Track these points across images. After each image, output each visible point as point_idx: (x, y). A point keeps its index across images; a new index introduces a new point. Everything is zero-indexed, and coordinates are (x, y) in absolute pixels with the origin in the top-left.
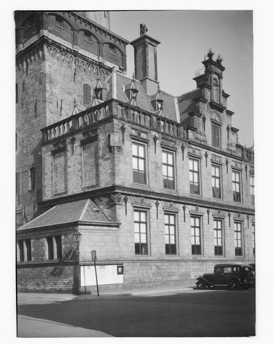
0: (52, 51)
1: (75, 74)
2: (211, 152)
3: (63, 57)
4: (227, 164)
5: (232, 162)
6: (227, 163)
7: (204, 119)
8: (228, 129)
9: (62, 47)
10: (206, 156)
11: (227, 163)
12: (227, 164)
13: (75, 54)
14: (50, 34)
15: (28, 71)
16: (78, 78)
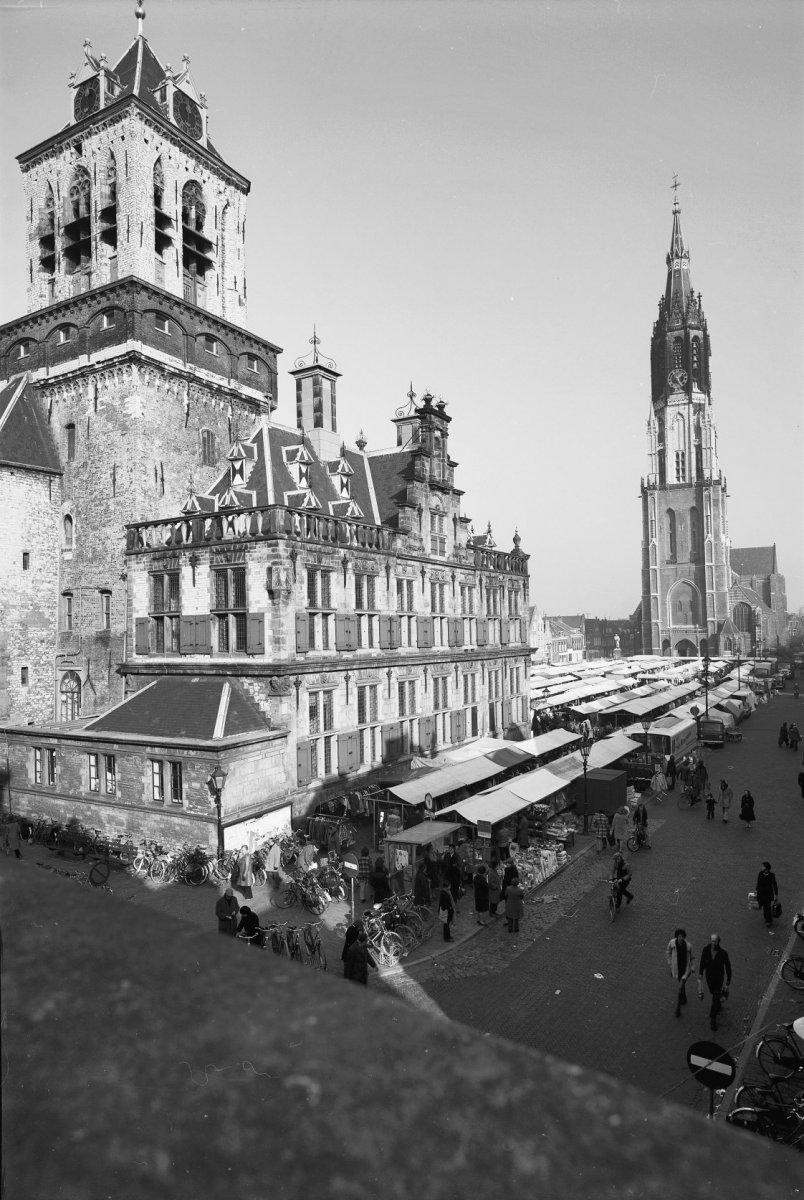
0: (147, 377)
1: (188, 414)
2: (429, 566)
3: (167, 386)
4: (453, 581)
5: (460, 575)
6: (453, 577)
7: (420, 511)
8: (454, 520)
9: (166, 367)
10: (423, 573)
11: (453, 577)
12: (453, 581)
13: (192, 379)
14: (145, 346)
15: (98, 406)
16: (194, 420)
